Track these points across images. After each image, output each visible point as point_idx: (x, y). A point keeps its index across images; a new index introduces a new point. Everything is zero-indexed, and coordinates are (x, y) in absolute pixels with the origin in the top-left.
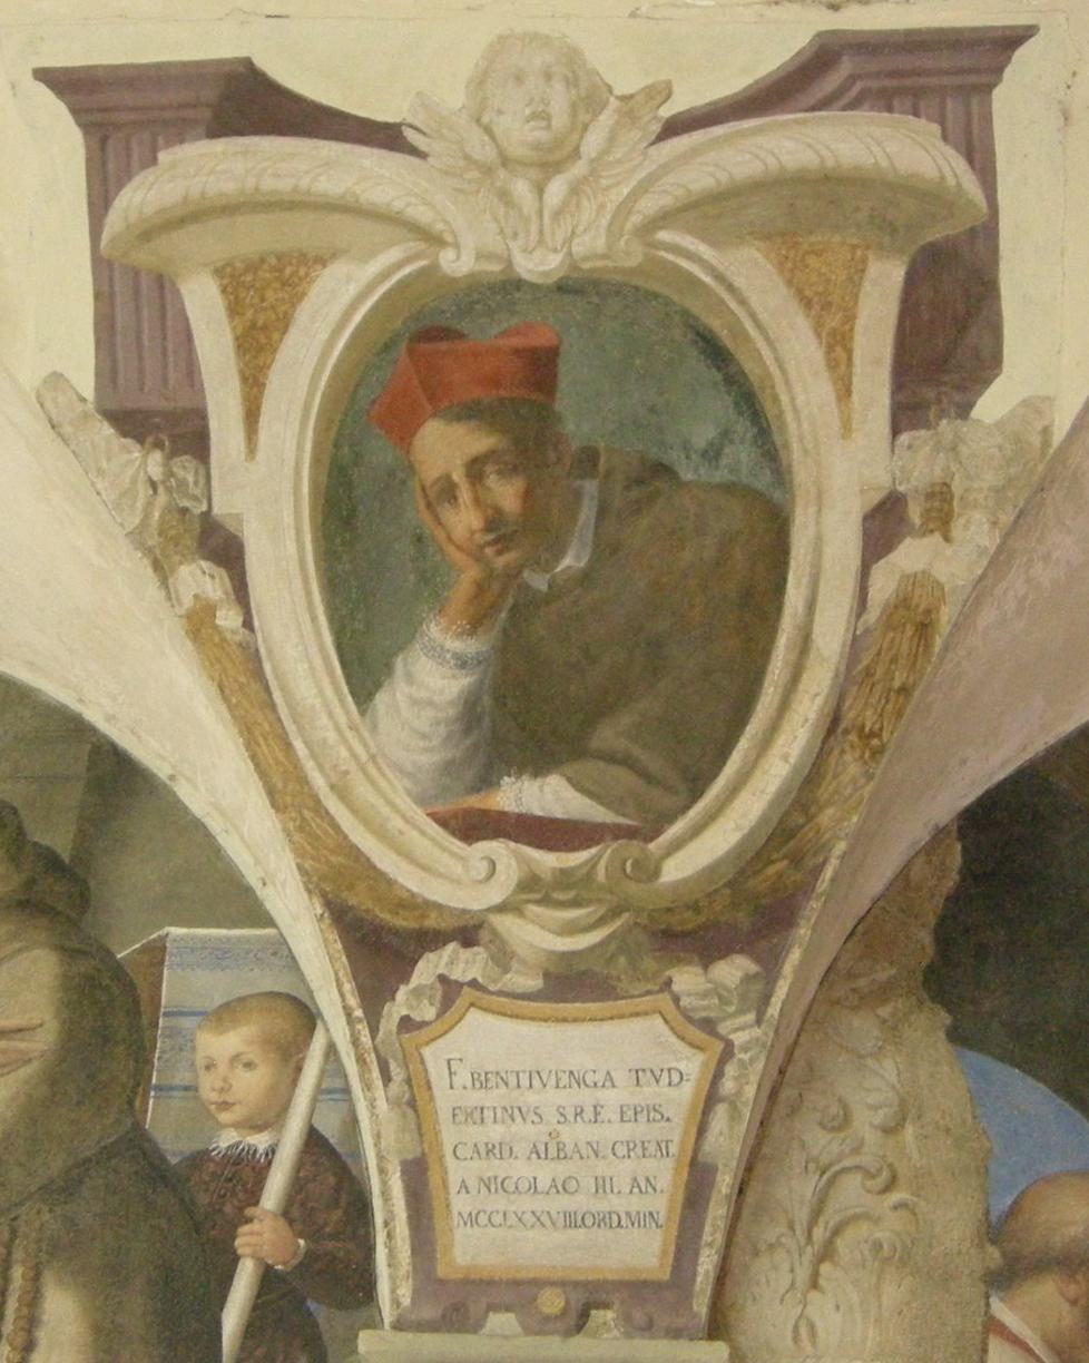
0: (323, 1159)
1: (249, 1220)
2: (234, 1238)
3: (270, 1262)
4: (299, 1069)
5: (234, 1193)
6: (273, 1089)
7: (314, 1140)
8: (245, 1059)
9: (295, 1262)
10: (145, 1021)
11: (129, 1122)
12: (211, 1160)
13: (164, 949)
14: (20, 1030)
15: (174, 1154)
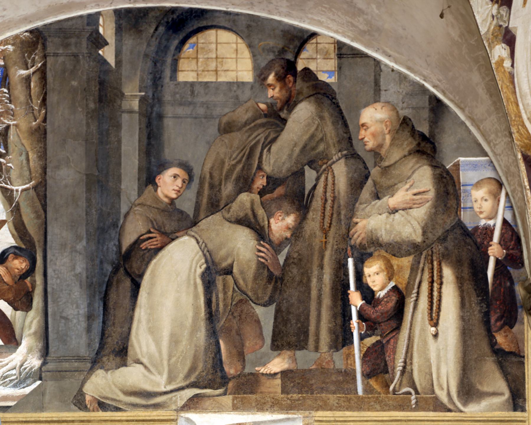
0: (508, 227)
1: (491, 246)
2: (487, 250)
3: (497, 257)
4: (499, 201)
5: (486, 238)
6: (493, 207)
7: (505, 222)
8: (485, 198)
9: (504, 256)
10: (457, 188)
11: (457, 218)
12: (479, 229)
13: (459, 165)
14: (424, 192)
15: (470, 227)
